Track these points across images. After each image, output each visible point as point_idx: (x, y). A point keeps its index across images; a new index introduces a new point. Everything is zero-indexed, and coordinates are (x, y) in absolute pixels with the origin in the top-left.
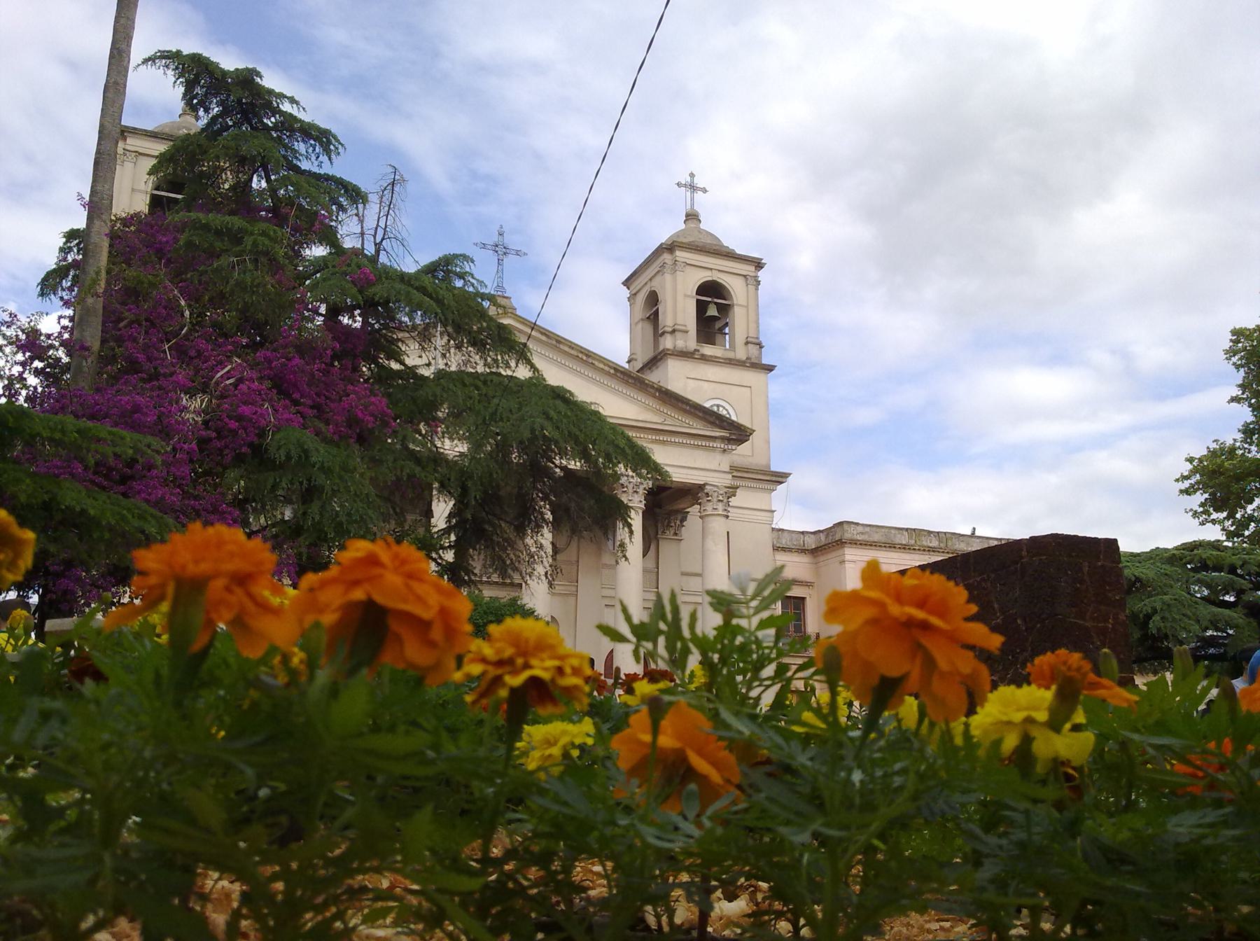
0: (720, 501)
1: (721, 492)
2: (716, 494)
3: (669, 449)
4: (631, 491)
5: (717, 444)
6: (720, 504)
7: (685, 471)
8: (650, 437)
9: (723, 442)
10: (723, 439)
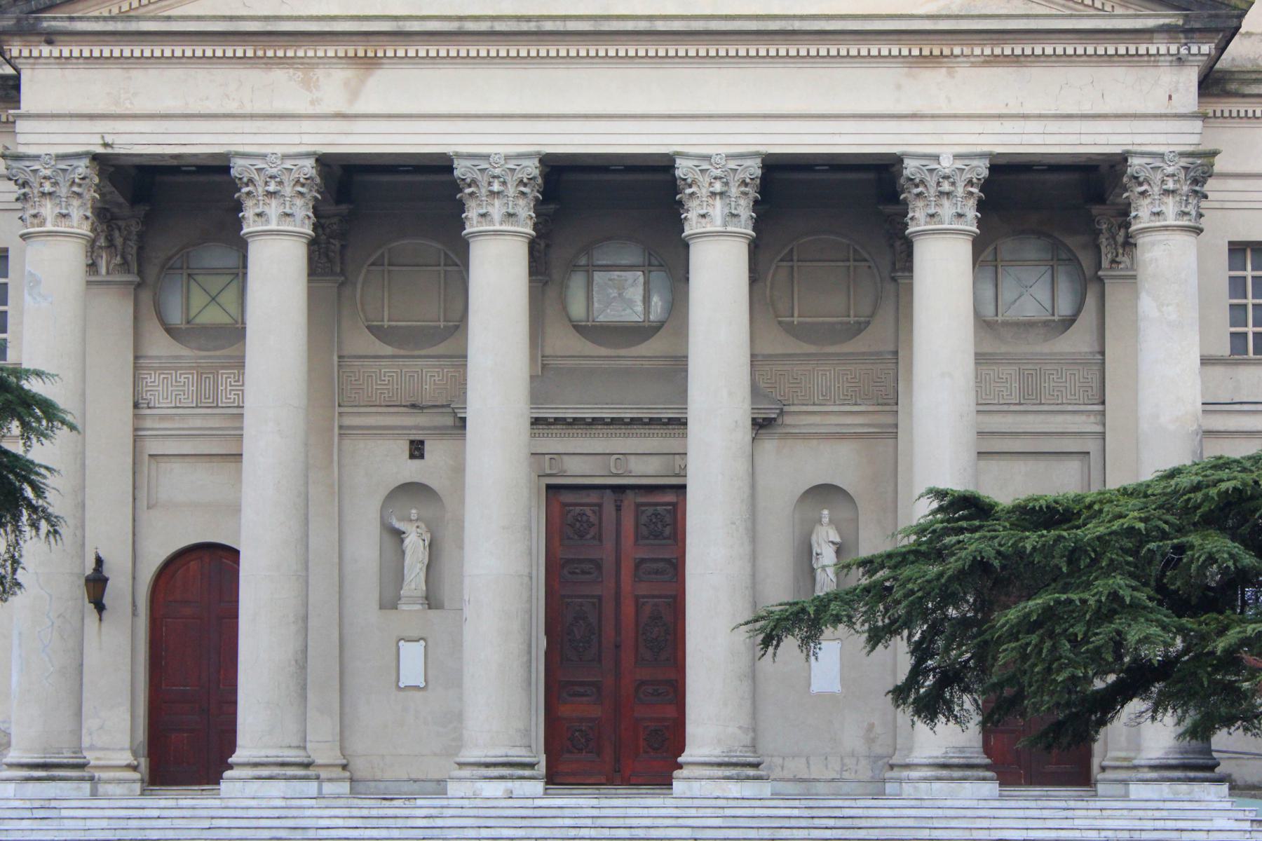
0: (1167, 192)
1: (1170, 170)
2: (1159, 176)
3: (1036, 73)
4: (932, 191)
5: (1161, 46)
6: (1170, 200)
7: (1076, 126)
8: (977, 51)
9: (1173, 40)
10: (1169, 31)
